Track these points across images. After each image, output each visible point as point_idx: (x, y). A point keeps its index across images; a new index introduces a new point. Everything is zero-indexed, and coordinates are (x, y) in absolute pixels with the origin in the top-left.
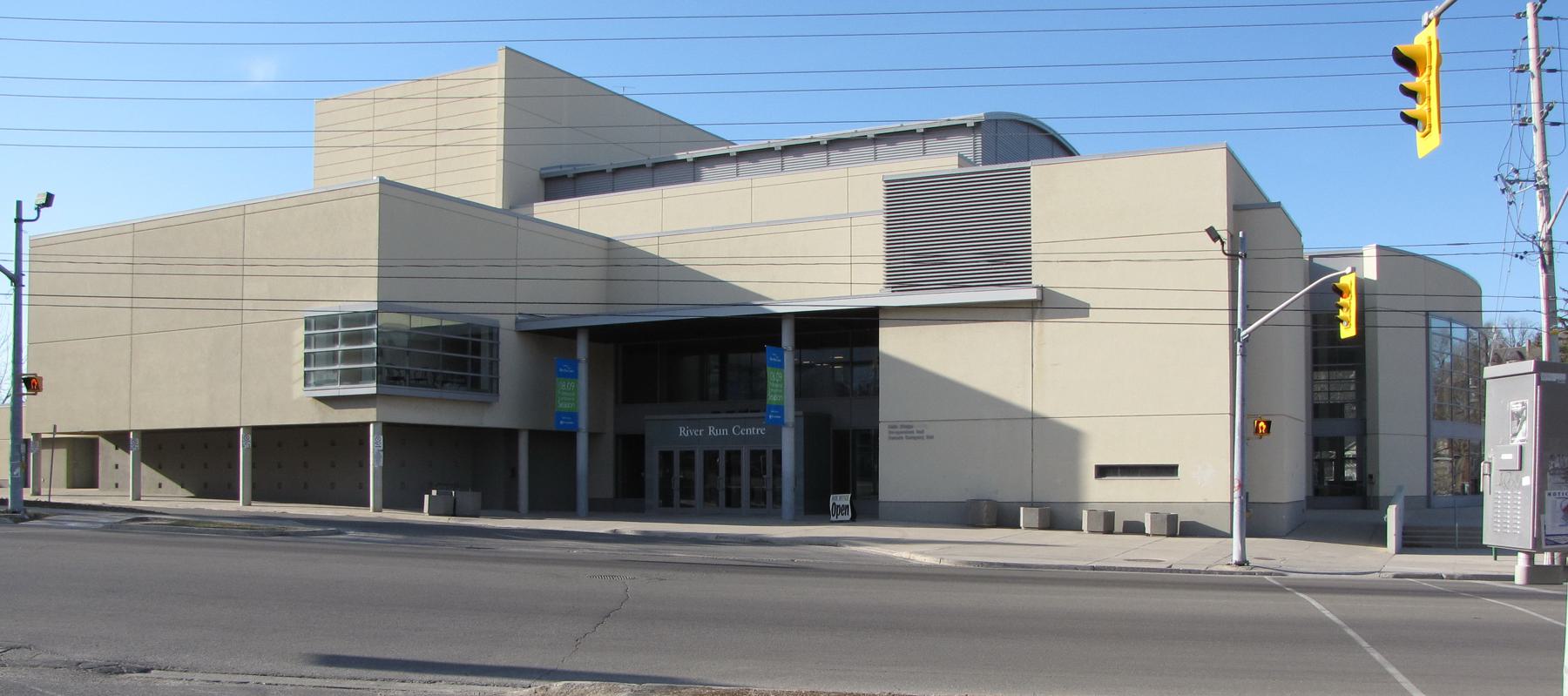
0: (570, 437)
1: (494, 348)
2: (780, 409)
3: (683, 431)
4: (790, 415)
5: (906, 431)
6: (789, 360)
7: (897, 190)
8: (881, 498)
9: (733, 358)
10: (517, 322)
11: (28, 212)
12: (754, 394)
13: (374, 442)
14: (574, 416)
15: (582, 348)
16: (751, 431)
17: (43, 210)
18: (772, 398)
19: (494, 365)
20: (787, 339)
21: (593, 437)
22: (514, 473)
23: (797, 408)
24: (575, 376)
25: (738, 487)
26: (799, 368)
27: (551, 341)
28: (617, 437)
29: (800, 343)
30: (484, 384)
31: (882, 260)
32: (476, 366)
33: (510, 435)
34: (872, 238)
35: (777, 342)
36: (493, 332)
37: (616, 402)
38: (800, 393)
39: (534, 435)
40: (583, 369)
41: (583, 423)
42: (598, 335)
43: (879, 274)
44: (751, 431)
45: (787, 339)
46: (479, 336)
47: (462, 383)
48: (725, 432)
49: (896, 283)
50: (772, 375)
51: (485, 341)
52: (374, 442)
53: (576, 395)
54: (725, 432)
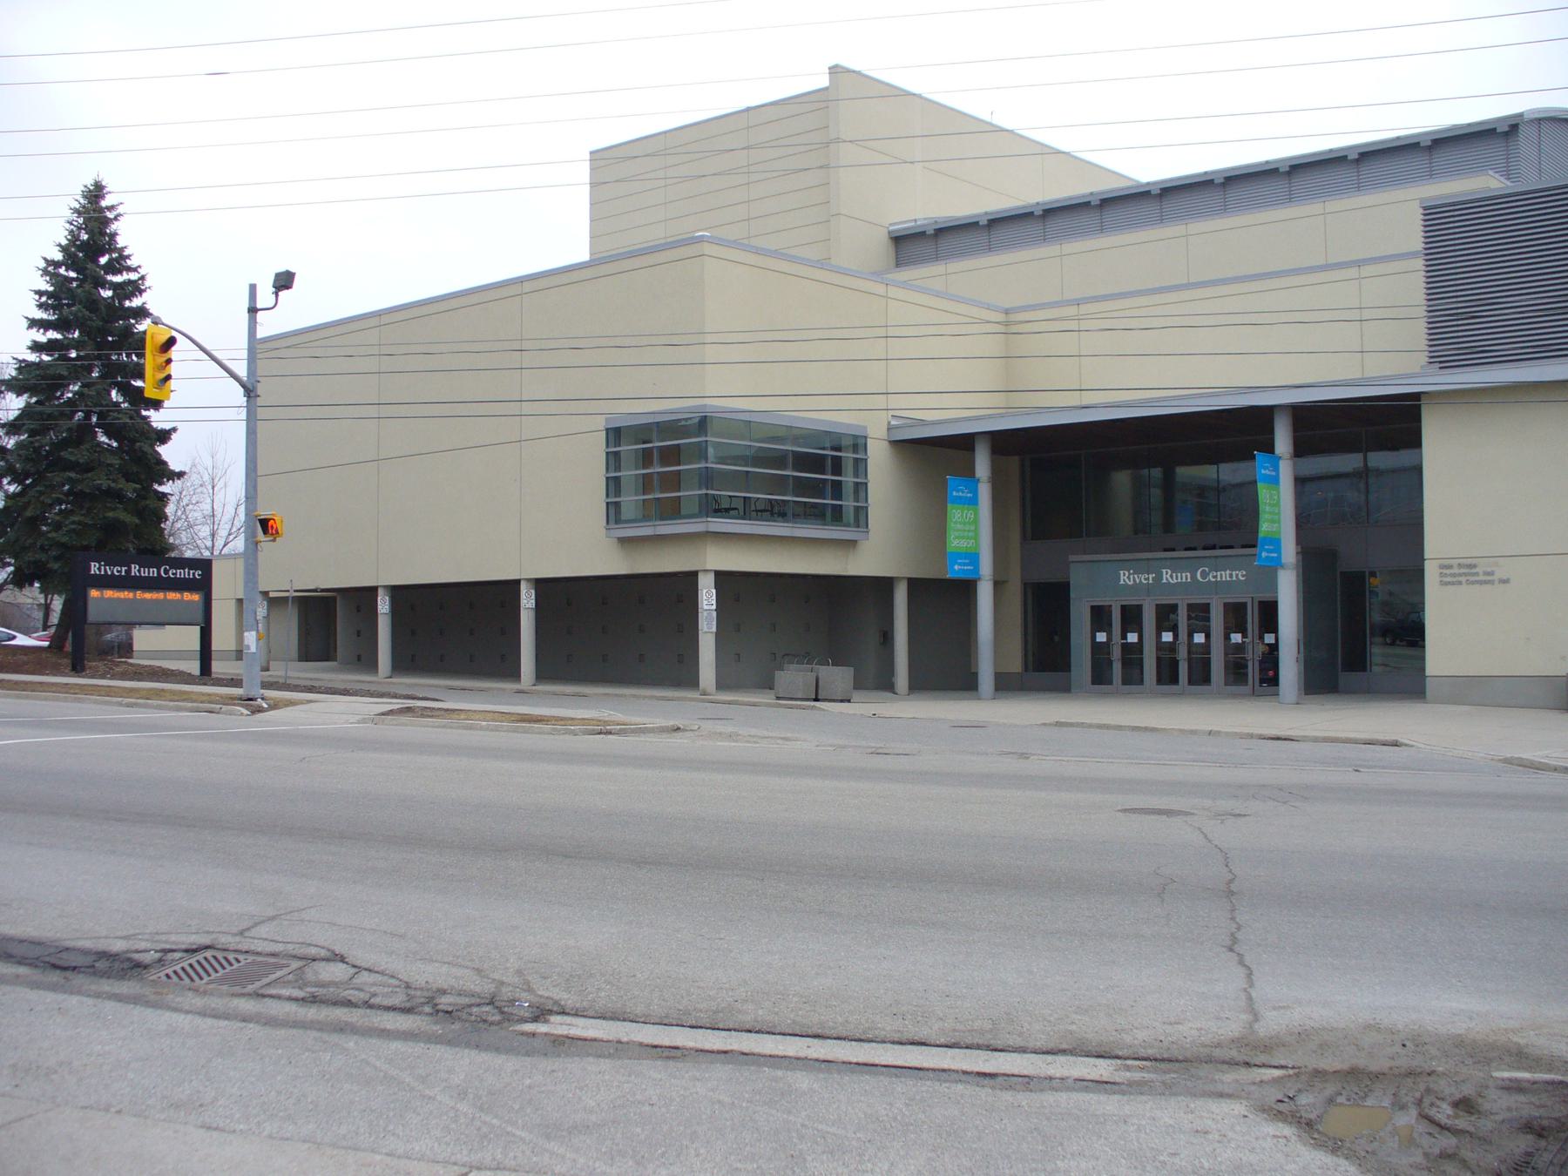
0: (965, 589)
1: (860, 465)
2: (1276, 543)
3: (1125, 578)
4: (1289, 551)
5: (1465, 572)
6: (1286, 471)
7: (1436, 217)
8: (1428, 672)
9: (1184, 472)
10: (890, 428)
11: (265, 297)
12: (1231, 526)
13: (708, 598)
14: (974, 558)
15: (982, 464)
16: (1224, 576)
17: (283, 294)
18: (1264, 528)
19: (861, 489)
20: (1283, 441)
21: (998, 585)
22: (887, 637)
23: (1299, 541)
24: (973, 501)
25: (1216, 656)
26: (1300, 482)
27: (936, 456)
28: (1025, 585)
29: (1301, 449)
30: (849, 515)
31: (1422, 311)
32: (837, 489)
33: (883, 586)
34: (1408, 287)
35: (1269, 448)
36: (859, 443)
37: (1024, 538)
38: (1303, 521)
39: (914, 585)
40: (984, 492)
41: (986, 568)
42: (1006, 443)
43: (1417, 334)
44: (1224, 576)
45: (1283, 441)
46: (838, 449)
47: (816, 514)
48: (1185, 577)
49: (1442, 358)
50: (1263, 492)
51: (848, 455)
52: (708, 598)
53: (973, 531)
54: (1185, 577)
